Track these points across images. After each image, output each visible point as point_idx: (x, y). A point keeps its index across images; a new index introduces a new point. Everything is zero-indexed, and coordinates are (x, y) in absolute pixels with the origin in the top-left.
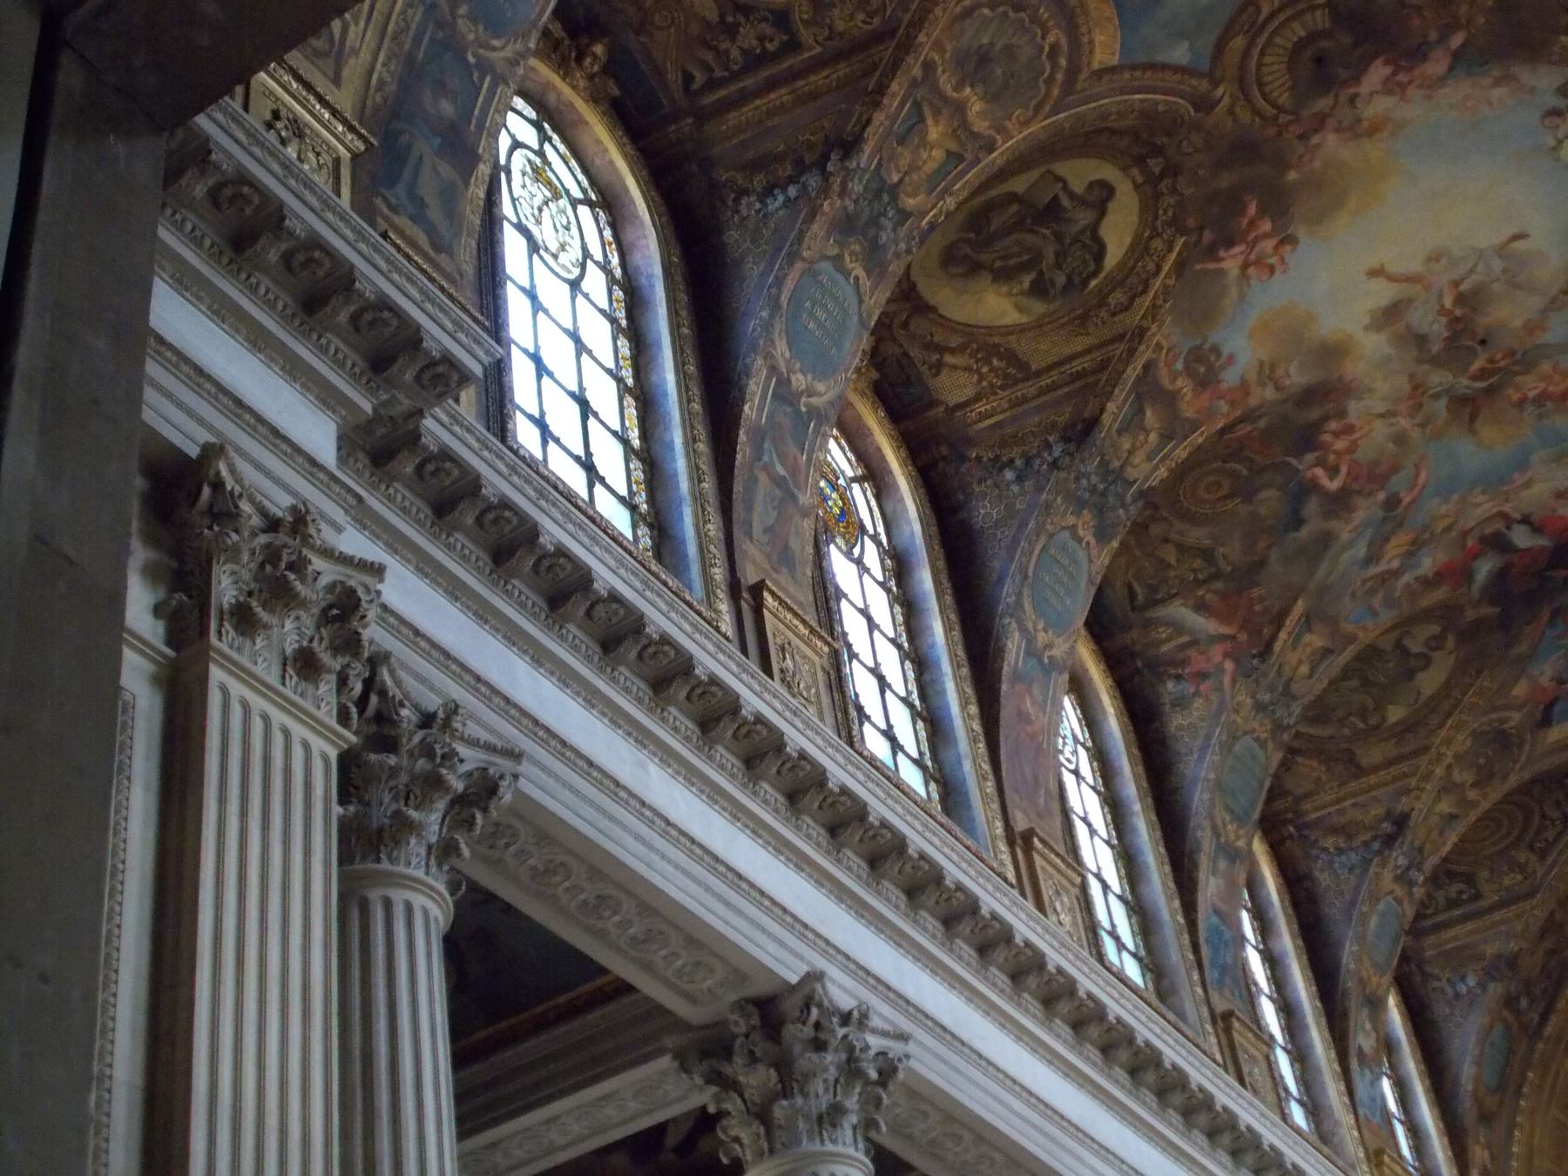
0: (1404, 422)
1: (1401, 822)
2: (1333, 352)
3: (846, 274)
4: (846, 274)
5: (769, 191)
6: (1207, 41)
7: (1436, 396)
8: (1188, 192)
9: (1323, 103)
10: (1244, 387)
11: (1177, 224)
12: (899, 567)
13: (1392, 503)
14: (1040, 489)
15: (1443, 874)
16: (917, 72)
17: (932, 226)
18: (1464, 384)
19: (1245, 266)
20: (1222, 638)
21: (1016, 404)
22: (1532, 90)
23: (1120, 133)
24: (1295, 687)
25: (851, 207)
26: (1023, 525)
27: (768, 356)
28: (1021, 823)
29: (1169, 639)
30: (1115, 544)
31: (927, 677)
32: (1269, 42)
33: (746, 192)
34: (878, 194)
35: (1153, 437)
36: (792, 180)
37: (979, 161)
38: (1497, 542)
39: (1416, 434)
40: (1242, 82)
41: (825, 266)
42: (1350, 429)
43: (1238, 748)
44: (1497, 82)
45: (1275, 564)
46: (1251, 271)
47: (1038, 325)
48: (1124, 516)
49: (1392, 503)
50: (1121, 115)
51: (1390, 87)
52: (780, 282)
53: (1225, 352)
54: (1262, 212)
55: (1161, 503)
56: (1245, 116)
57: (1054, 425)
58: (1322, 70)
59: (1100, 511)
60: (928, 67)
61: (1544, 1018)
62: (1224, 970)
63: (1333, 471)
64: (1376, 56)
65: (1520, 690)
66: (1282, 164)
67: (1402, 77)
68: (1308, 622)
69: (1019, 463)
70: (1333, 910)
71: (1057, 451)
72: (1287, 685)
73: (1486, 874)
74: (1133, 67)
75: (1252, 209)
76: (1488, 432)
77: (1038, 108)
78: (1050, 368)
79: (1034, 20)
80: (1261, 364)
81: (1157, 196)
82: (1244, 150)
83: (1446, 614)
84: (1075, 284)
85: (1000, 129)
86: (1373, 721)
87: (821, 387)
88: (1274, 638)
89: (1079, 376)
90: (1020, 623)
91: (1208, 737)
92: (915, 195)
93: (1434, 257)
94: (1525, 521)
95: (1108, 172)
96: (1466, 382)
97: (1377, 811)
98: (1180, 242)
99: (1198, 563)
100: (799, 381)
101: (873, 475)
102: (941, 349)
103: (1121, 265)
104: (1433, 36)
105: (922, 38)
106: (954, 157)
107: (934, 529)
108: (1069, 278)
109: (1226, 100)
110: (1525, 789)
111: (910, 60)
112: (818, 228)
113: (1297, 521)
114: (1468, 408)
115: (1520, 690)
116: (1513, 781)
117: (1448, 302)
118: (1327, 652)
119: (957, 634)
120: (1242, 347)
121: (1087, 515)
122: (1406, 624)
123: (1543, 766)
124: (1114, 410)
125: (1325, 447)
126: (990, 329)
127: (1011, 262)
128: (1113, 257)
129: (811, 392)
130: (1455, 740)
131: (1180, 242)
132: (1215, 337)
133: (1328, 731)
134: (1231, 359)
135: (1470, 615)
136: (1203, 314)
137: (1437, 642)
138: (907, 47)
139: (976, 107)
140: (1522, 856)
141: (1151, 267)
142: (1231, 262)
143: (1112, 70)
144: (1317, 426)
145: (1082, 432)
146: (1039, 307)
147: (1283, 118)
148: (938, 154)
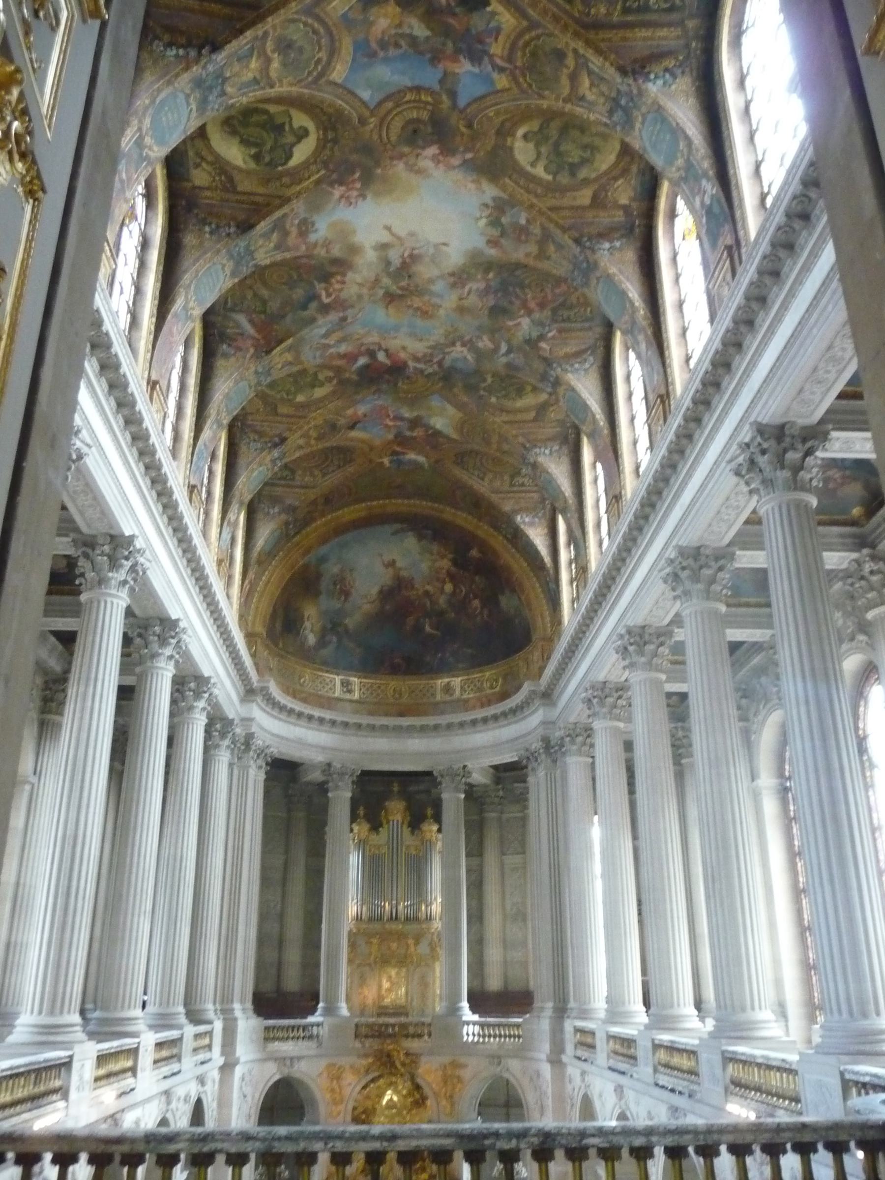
0: (365, 291)
1: (283, 440)
2: (354, 249)
3: (188, 104)
4: (188, 104)
5: (169, 45)
6: (378, 97)
7: (382, 288)
8: (337, 153)
9: (406, 149)
10: (315, 245)
11: (325, 164)
12: (145, 244)
13: (344, 319)
14: (218, 241)
15: (286, 467)
16: (260, 33)
17: (232, 105)
18: (394, 288)
19: (342, 197)
20: (253, 338)
21: (222, 200)
22: (484, 192)
23: (325, 114)
24: (272, 371)
25: (204, 75)
26: (205, 253)
27: (140, 122)
28: (154, 377)
29: (233, 328)
30: (236, 280)
31: (138, 297)
32: (400, 112)
33: (160, 40)
34: (217, 77)
35: (272, 245)
36: (182, 46)
37: (263, 88)
38: (372, 354)
39: (366, 298)
40: (382, 120)
41: (181, 96)
42: (343, 283)
43: (241, 384)
44: (473, 181)
45: (289, 319)
46: (343, 200)
47: (248, 173)
48: (245, 271)
49: (344, 319)
50: (330, 105)
51: (434, 158)
52: (159, 91)
53: (317, 226)
54: (360, 179)
55: (260, 273)
56: (375, 137)
57: (234, 218)
58: (414, 136)
59: (238, 264)
60: (266, 34)
61: (296, 534)
62: (198, 468)
63: (329, 295)
64: (436, 143)
65: (350, 412)
66: (378, 164)
67: (441, 158)
68: (289, 349)
69: (213, 226)
70: (242, 461)
71: (232, 230)
72: (269, 370)
73: (300, 472)
74: (345, 88)
75: (357, 175)
76: (391, 310)
77: (300, 81)
78: (245, 193)
79: (319, 42)
80: (326, 239)
81: (324, 147)
82: (367, 149)
83: (338, 370)
84: (272, 164)
85: (280, 81)
86: (290, 397)
87: (155, 148)
88: (274, 348)
89: (253, 203)
90: (187, 293)
91: (231, 375)
92: (232, 86)
93: (412, 234)
94: (386, 351)
95: (311, 126)
96: (395, 288)
97: (278, 432)
98: (323, 172)
99: (258, 304)
100: (148, 140)
101: (149, 196)
102: (202, 158)
103: (295, 168)
104: (461, 149)
105: (270, 19)
106: (256, 81)
107: (166, 234)
108: (272, 159)
109: (372, 126)
110: (332, 449)
111: (260, 25)
112: (186, 77)
113: (305, 307)
114: (390, 298)
115: (350, 412)
116: (328, 444)
117: (406, 255)
118: (290, 363)
119: (159, 285)
120: (323, 228)
121: (231, 263)
122: (322, 367)
123: (342, 443)
124: (263, 226)
125: (331, 285)
126: (228, 163)
127: (251, 139)
128: (294, 162)
129: (150, 149)
130: (317, 418)
131: (323, 172)
132: (315, 218)
133: (273, 393)
134: (316, 231)
135: (347, 375)
136: (316, 207)
137: (329, 380)
138: (262, 18)
139: (275, 65)
140: (316, 472)
141: (306, 176)
142: (338, 191)
143: (336, 84)
144: (332, 275)
145: (245, 227)
146: (252, 165)
147: (389, 146)
148: (250, 75)
